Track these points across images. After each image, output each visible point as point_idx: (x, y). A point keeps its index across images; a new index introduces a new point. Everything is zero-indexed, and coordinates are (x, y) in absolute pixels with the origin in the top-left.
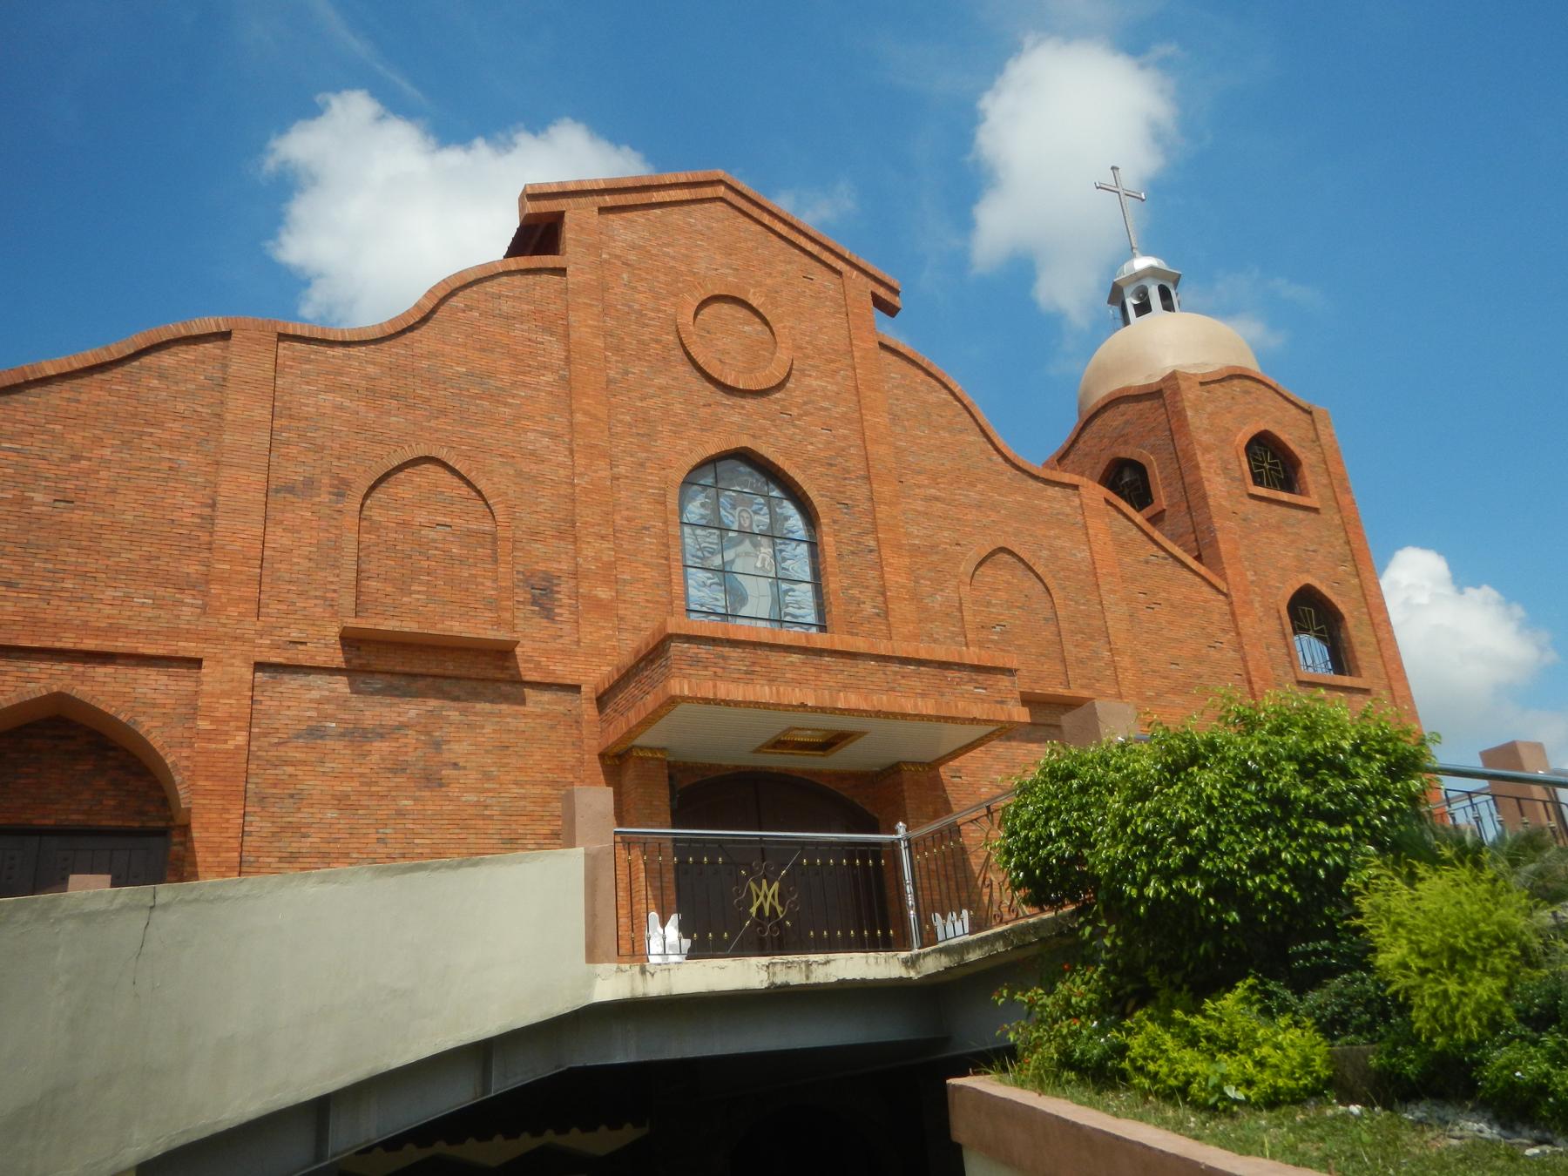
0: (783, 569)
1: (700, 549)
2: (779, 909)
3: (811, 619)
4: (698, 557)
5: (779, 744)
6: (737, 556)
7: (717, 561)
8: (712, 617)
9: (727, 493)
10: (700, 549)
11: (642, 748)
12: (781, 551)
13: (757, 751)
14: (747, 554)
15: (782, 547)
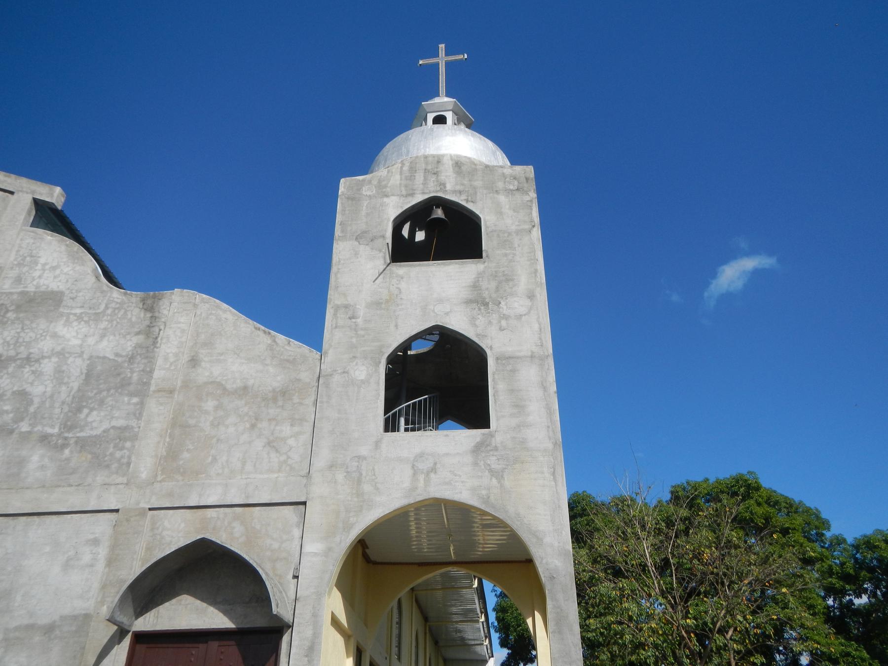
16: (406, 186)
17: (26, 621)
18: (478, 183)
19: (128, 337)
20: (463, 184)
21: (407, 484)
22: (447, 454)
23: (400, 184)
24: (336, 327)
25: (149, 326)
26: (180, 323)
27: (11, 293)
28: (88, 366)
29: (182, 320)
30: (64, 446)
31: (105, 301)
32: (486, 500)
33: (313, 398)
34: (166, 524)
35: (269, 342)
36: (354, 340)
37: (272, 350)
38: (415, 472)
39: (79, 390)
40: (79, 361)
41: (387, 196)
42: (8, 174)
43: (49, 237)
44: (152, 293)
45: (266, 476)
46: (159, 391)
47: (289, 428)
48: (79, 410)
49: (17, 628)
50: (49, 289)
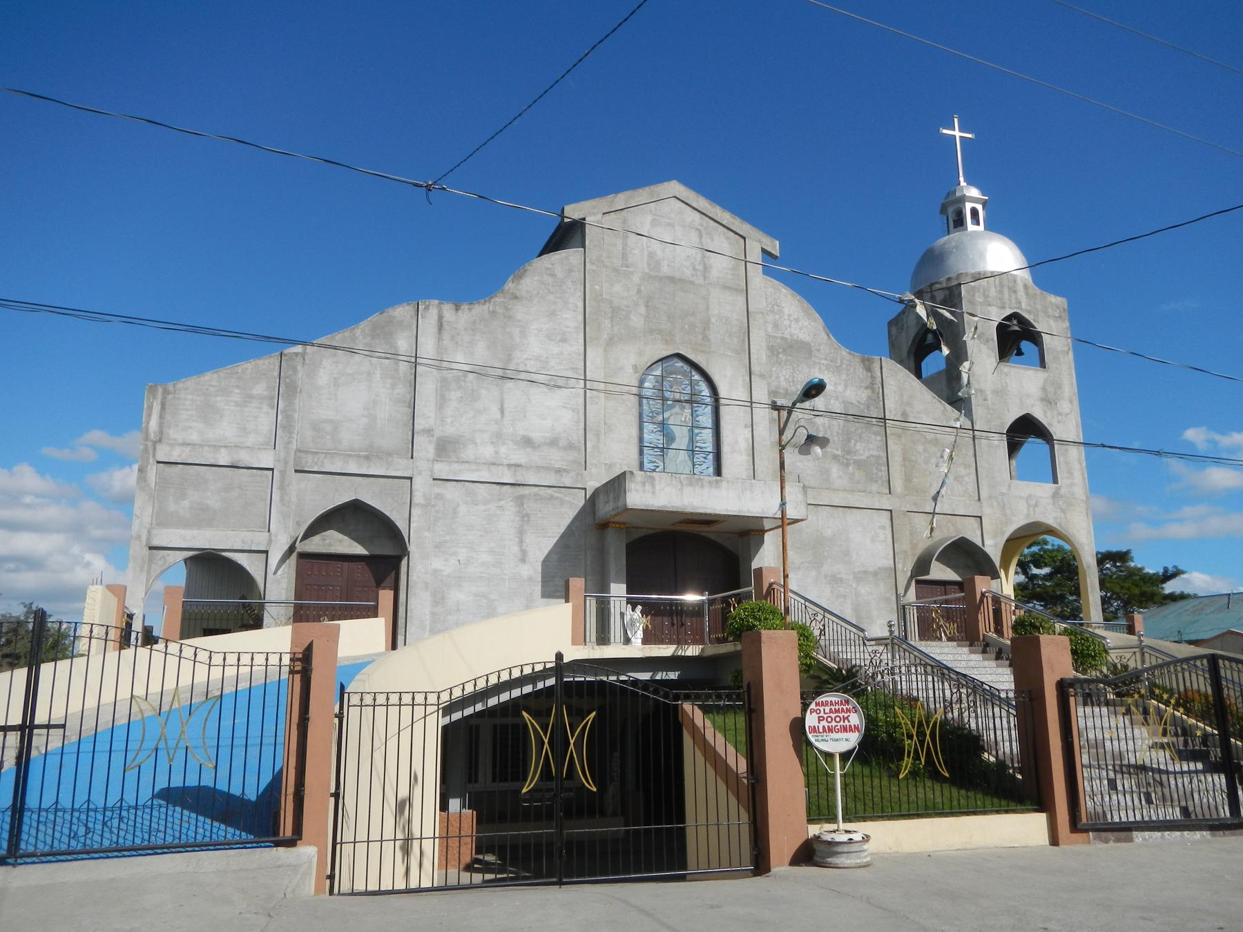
0: (697, 421)
1: (652, 412)
2: (650, 626)
3: (710, 449)
4: (650, 417)
5: (681, 522)
6: (671, 415)
7: (660, 418)
8: (656, 450)
9: (668, 379)
10: (652, 412)
11: (614, 523)
12: (696, 411)
13: (673, 524)
14: (677, 414)
15: (696, 409)
16: (1000, 299)
17: (864, 569)
18: (1039, 307)
19: (862, 389)
20: (1030, 305)
21: (1025, 512)
22: (1041, 497)
23: (996, 296)
24: (978, 405)
25: (871, 383)
26: (891, 385)
27: (774, 337)
28: (844, 408)
29: (892, 383)
30: (847, 465)
31: (839, 357)
32: (1060, 526)
33: (972, 452)
34: (916, 521)
35: (942, 408)
36: (988, 416)
37: (945, 415)
38: (1029, 506)
39: (844, 426)
40: (837, 403)
41: (990, 305)
42: (733, 215)
43: (783, 290)
44: (866, 356)
45: (957, 498)
46: (892, 434)
47: (963, 470)
48: (849, 440)
49: (859, 572)
50: (800, 339)
